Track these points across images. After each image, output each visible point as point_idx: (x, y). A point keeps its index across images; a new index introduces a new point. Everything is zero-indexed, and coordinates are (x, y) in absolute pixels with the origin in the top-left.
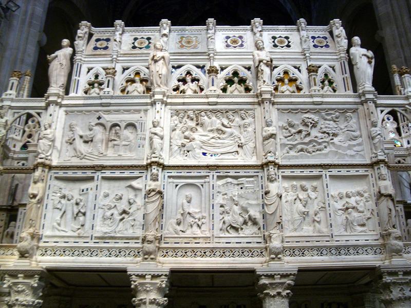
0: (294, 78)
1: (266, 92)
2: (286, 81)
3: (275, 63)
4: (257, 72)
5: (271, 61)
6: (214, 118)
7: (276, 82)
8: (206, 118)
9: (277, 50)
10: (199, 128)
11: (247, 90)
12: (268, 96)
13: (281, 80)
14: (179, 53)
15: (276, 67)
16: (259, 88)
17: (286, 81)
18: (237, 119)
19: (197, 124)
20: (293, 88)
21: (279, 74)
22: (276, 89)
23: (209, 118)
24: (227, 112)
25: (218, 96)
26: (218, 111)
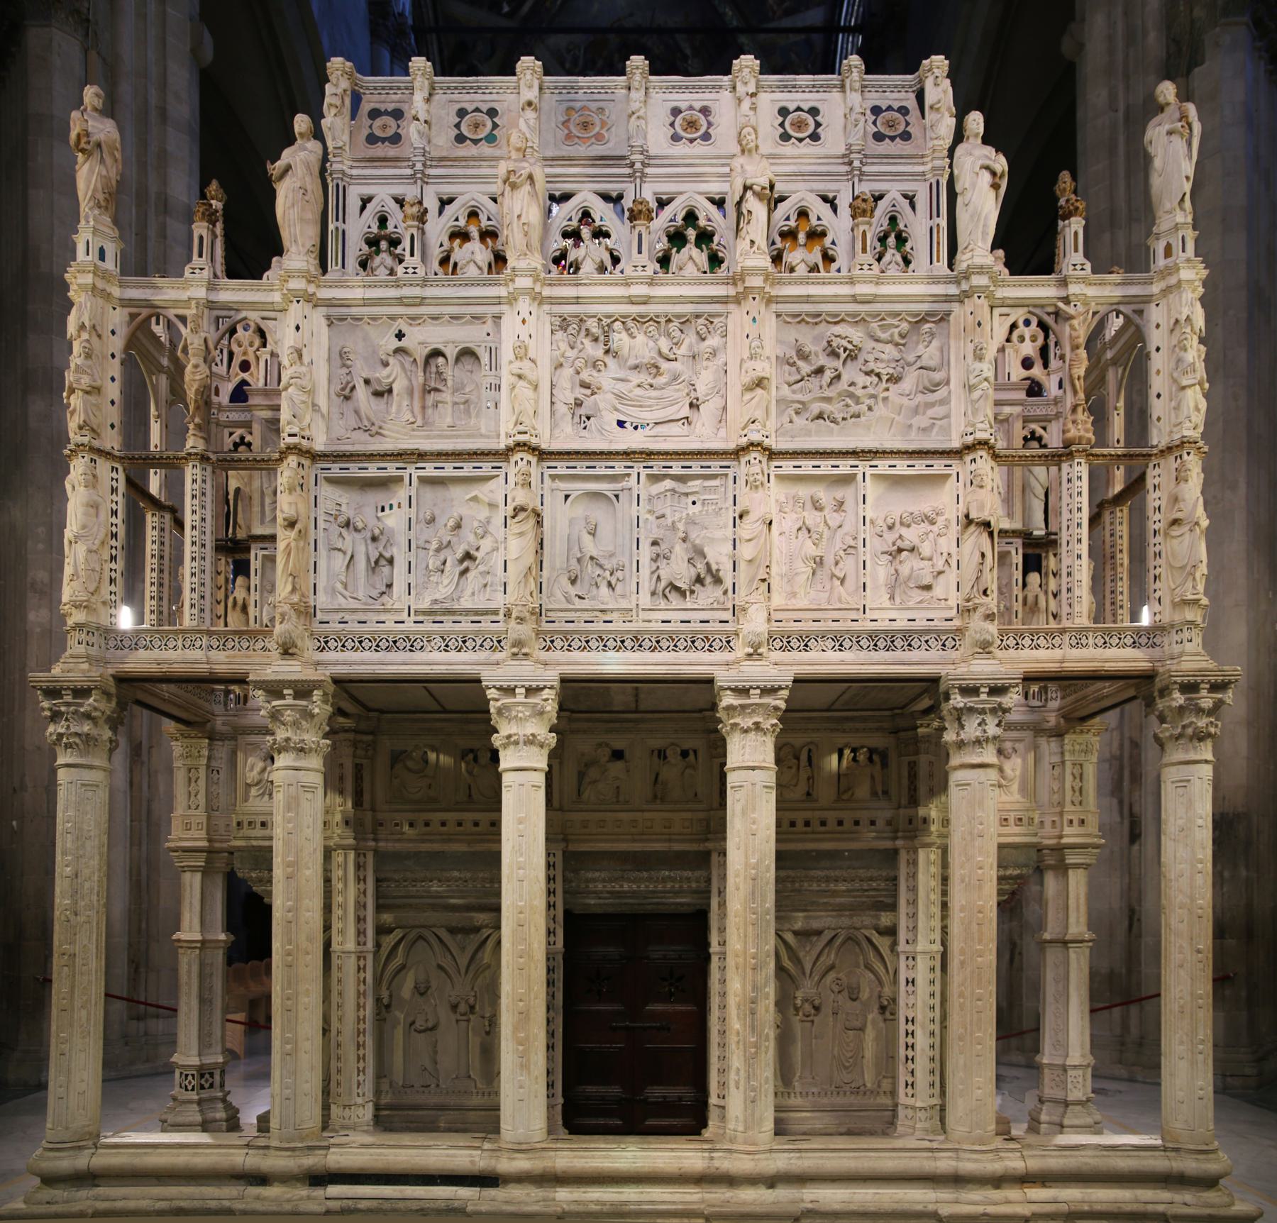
0: (819, 229)
1: (754, 271)
2: (802, 237)
3: (778, 187)
4: (739, 214)
5: (772, 187)
6: (641, 338)
7: (778, 239)
8: (624, 335)
9: (789, 149)
10: (609, 360)
11: (715, 260)
12: (756, 281)
13: (789, 235)
14: (563, 159)
15: (782, 199)
16: (741, 260)
17: (802, 237)
18: (690, 338)
19: (607, 352)
20: (816, 257)
21: (788, 219)
22: (777, 259)
23: (632, 336)
24: (669, 321)
25: (651, 282)
26: (651, 319)
